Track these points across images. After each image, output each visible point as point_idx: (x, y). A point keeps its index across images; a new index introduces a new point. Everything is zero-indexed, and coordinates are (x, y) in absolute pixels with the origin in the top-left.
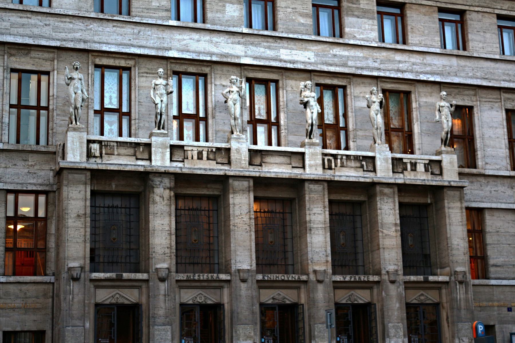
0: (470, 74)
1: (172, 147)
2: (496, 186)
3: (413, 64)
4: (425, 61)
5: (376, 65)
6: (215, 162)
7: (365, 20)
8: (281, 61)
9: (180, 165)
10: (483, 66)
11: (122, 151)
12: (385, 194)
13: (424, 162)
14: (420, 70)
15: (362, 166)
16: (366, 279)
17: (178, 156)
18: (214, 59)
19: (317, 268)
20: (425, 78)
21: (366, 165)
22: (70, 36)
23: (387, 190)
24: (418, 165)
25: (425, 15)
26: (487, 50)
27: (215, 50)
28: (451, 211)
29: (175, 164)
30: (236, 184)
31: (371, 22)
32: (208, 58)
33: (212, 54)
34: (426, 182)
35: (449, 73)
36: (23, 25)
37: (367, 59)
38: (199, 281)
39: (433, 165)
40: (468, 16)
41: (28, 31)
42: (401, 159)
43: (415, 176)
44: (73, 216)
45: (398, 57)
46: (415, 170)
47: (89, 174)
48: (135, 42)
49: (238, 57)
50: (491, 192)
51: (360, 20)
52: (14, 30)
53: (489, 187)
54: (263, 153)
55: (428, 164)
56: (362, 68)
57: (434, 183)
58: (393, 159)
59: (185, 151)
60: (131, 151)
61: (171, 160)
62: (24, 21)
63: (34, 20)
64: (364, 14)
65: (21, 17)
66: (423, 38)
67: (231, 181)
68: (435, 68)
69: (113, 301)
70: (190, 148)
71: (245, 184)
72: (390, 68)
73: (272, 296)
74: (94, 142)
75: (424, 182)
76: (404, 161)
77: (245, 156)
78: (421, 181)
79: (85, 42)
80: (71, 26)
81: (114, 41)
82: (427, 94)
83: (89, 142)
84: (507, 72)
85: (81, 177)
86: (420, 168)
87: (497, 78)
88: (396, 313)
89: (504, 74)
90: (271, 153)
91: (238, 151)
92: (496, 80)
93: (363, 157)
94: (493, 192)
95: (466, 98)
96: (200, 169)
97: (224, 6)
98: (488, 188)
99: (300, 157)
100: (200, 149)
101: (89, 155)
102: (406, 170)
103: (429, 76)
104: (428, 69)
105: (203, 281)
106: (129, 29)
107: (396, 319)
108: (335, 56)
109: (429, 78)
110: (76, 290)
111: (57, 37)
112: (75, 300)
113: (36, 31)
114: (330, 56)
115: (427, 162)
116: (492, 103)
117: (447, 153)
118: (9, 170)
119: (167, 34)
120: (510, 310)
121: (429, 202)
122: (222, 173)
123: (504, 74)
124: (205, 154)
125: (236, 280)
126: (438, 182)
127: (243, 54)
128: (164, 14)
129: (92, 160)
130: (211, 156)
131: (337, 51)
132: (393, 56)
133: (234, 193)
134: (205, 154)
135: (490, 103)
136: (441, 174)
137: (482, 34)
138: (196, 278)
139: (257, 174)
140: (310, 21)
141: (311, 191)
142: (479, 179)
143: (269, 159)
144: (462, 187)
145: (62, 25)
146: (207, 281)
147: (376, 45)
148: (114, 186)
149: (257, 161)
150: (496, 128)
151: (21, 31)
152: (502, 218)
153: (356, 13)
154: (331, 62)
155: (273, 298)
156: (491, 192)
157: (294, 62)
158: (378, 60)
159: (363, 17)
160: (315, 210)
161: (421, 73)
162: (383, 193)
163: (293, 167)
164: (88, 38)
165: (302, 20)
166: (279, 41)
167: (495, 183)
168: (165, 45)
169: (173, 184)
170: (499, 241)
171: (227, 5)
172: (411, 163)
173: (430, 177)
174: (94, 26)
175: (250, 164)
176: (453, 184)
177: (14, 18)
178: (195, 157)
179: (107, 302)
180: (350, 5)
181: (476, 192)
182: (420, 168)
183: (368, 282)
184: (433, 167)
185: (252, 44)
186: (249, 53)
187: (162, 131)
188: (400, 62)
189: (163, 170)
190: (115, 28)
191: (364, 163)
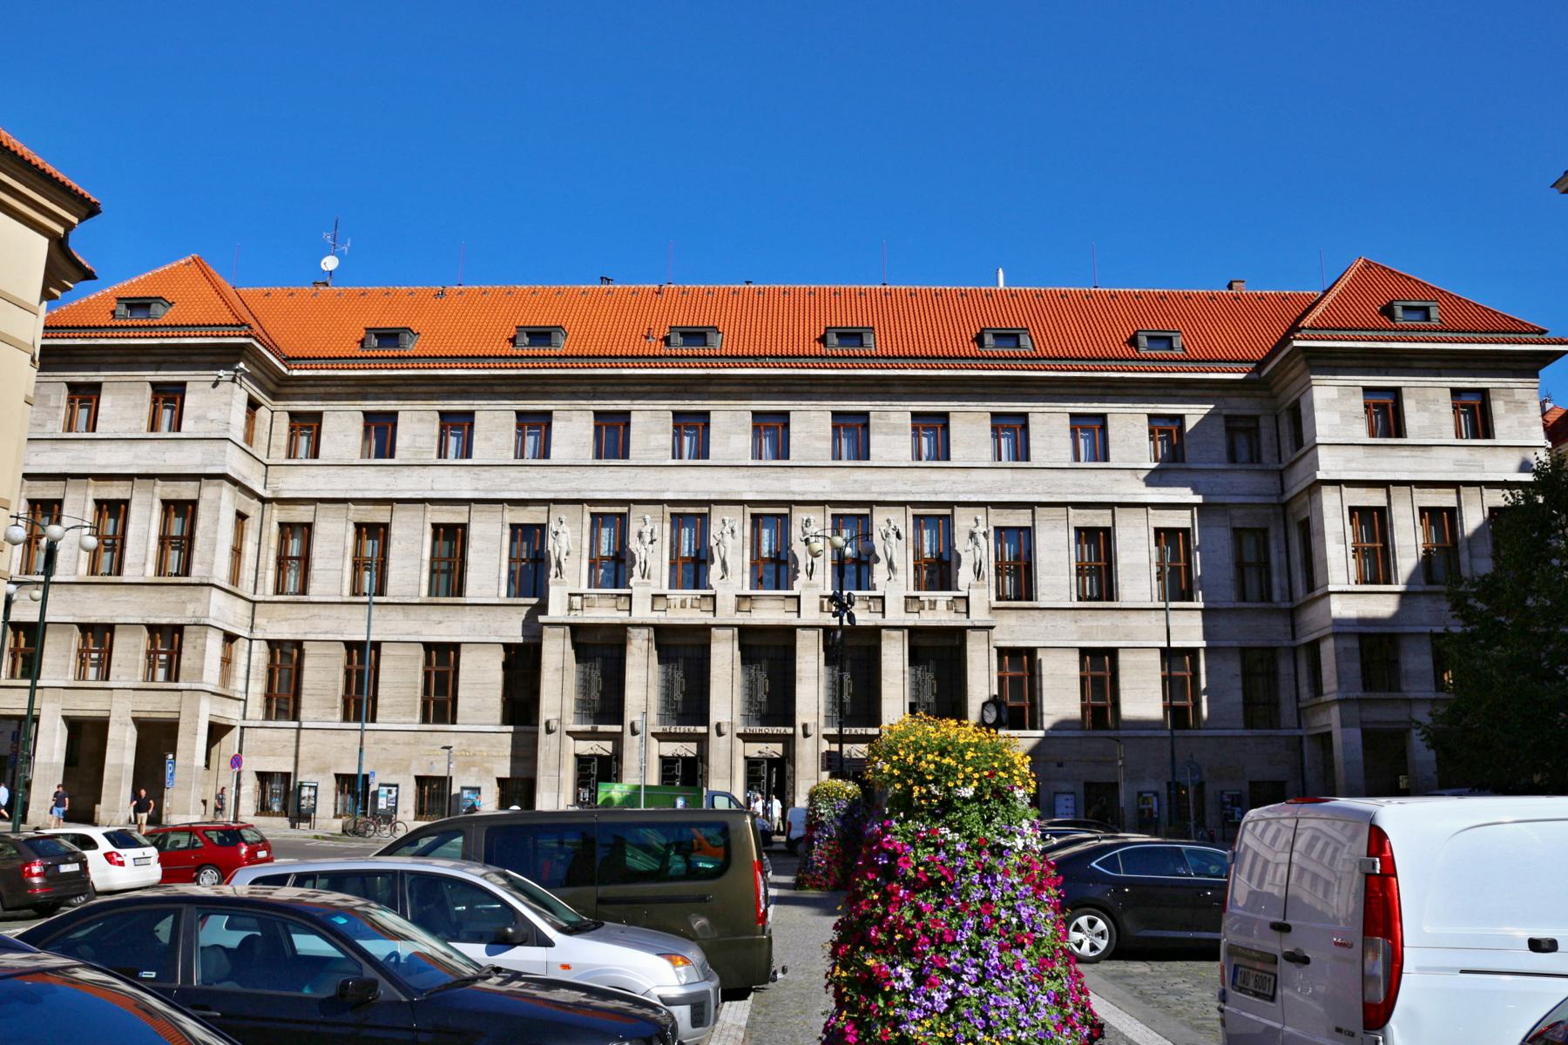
0: (1028, 489)
1: (654, 596)
4: (969, 478)
5: (907, 488)
7: (896, 437)
8: (793, 493)
9: (662, 614)
11: (604, 602)
12: (893, 638)
13: (946, 599)
14: (961, 490)
15: (869, 607)
16: (864, 732)
17: (660, 604)
18: (713, 497)
19: (806, 721)
20: (965, 499)
22: (566, 486)
24: (938, 603)
25: (973, 424)
27: (718, 487)
28: (974, 654)
29: (655, 614)
31: (902, 438)
32: (706, 498)
33: (709, 492)
35: (1000, 490)
36: (522, 479)
37: (895, 481)
38: (675, 733)
39: (957, 601)
40: (1031, 419)
41: (526, 486)
42: (918, 597)
43: (934, 615)
44: (552, 669)
45: (936, 475)
46: (934, 609)
47: (567, 628)
48: (631, 487)
49: (739, 492)
50: (1046, 628)
51: (889, 438)
52: (513, 486)
56: (885, 493)
57: (953, 624)
58: (906, 597)
60: (613, 602)
61: (653, 610)
62: (524, 475)
63: (533, 472)
64: (895, 429)
67: (713, 629)
69: (592, 752)
70: (673, 597)
71: (729, 632)
72: (924, 490)
74: (576, 595)
76: (921, 599)
77: (732, 601)
79: (579, 491)
80: (568, 475)
81: (609, 488)
83: (571, 595)
85: (560, 630)
86: (942, 605)
87: (1064, 491)
89: (1074, 485)
91: (724, 596)
92: (1059, 493)
93: (871, 597)
95: (1022, 517)
96: (679, 619)
97: (729, 438)
98: (1044, 623)
99: (796, 600)
100: (684, 597)
101: (571, 609)
102: (923, 609)
103: (969, 496)
104: (973, 487)
105: (680, 734)
106: (625, 472)
108: (856, 481)
110: (552, 742)
111: (553, 489)
112: (552, 750)
113: (534, 485)
115: (950, 599)
117: (977, 587)
118: (505, 624)
119: (666, 473)
120: (1060, 765)
121: (957, 643)
122: (702, 622)
123: (1074, 485)
124: (689, 602)
125: (713, 732)
127: (748, 489)
128: (663, 453)
129: (573, 613)
130: (696, 604)
131: (859, 474)
133: (718, 641)
134: (689, 602)
136: (968, 612)
137: (1048, 439)
138: (673, 731)
139: (741, 623)
140: (829, 445)
141: (804, 637)
142: (1032, 612)
143: (758, 604)
144: (992, 627)
145: (559, 475)
146: (684, 734)
147: (906, 465)
148: (599, 637)
149: (746, 606)
150: (1059, 551)
151: (520, 486)
153: (884, 430)
154: (850, 489)
155: (760, 752)
156: (1046, 628)
157: (803, 493)
158: (909, 483)
159: (893, 434)
160: (807, 658)
161: (959, 493)
164: (584, 487)
165: (818, 444)
168: (663, 487)
169: (652, 635)
171: (732, 436)
172: (930, 601)
173: (953, 615)
174: (591, 472)
175: (738, 610)
176: (977, 624)
177: (513, 472)
178: (678, 606)
179: (587, 753)
180: (878, 421)
182: (942, 605)
183: (866, 735)
185: (758, 476)
186: (755, 487)
187: (646, 580)
188: (936, 481)
189: (639, 622)
191: (871, 604)
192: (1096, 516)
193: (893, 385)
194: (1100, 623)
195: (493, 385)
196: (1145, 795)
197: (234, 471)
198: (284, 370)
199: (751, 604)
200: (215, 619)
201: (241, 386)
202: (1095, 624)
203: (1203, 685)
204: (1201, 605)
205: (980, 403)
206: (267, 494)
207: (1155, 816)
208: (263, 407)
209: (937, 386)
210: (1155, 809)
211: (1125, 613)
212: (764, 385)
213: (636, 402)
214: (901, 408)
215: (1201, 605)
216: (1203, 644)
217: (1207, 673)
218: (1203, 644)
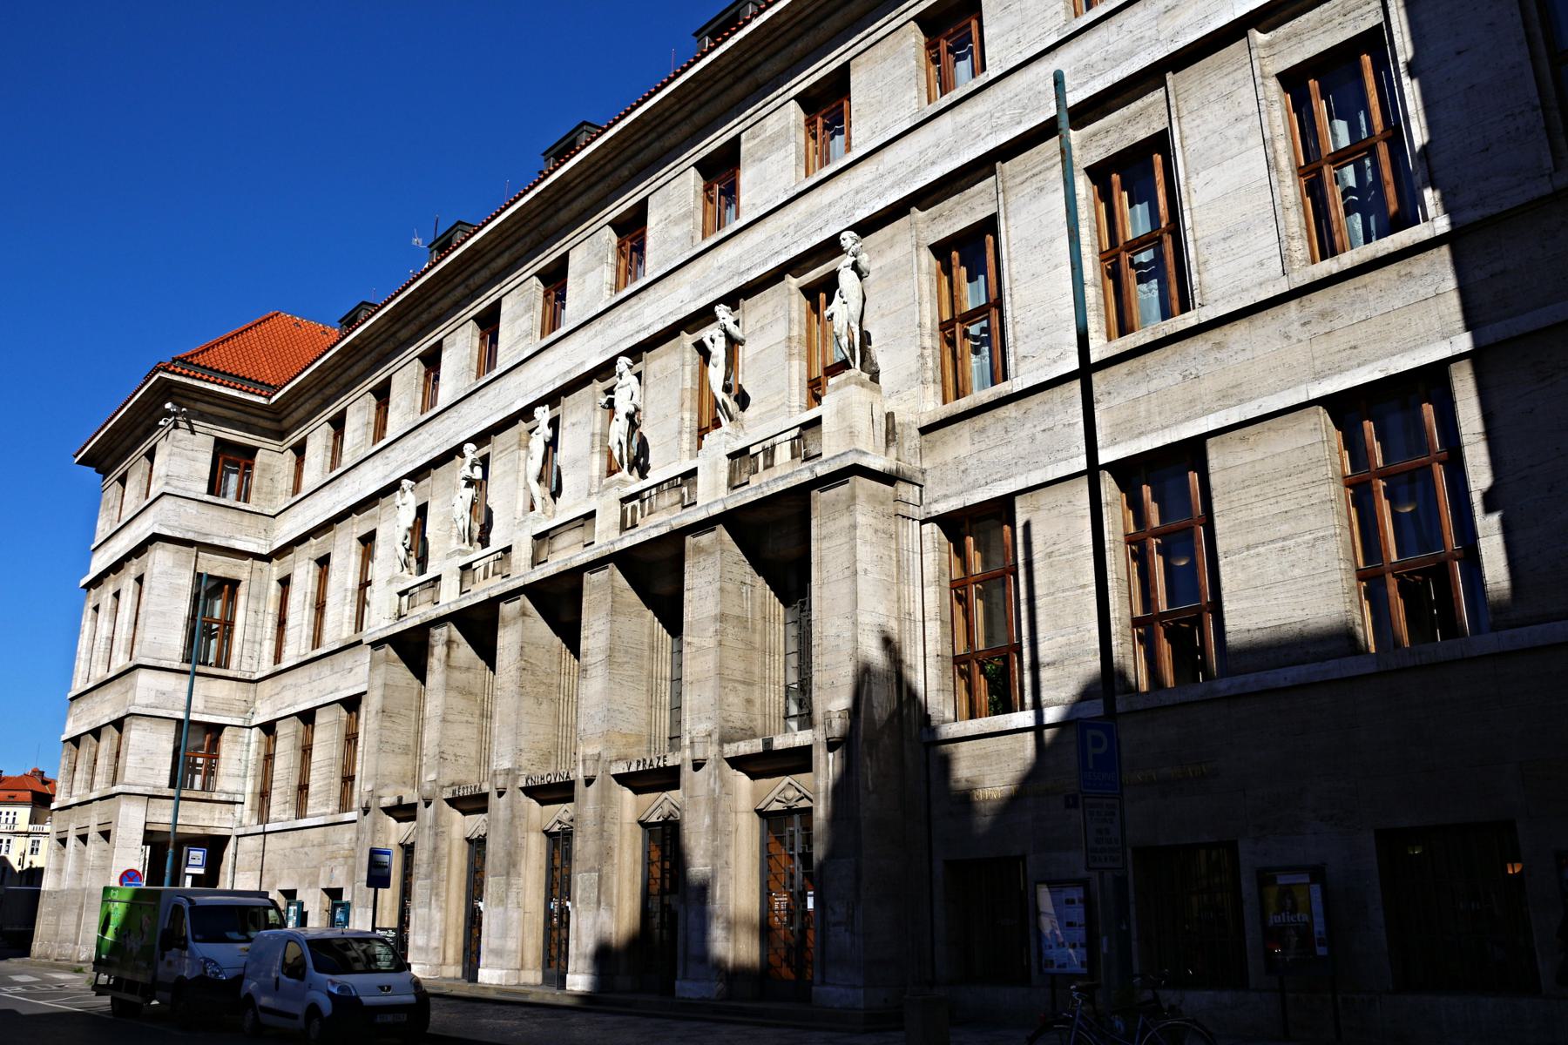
2: (1049, 413)
3: (857, 193)
6: (500, 576)
10: (1018, 90)
21: (689, 494)
23: (705, 539)
26: (1028, 40)
28: (825, 544)
30: (506, 609)
34: (765, 489)
46: (772, 465)
53: (1029, 425)
54: (551, 535)
55: (799, 437)
59: (475, 569)
65: (415, 438)
66: (877, 119)
68: (901, 172)
73: (556, 818)
75: (760, 491)
78: (754, 492)
82: (883, 247)
84: (1084, 62)
88: (703, 842)
90: (559, 530)
94: (1039, 436)
107: (702, 857)
108: (720, 268)
109: (873, 208)
114: (713, 274)
115: (794, 433)
116: (1041, 177)
126: (789, 480)
132: (818, 200)
135: (1034, 180)
142: (1001, 412)
152: (1063, 510)
155: (560, 822)
156: (1033, 439)
162: (699, 547)
163: (585, 546)
166: (643, 295)
167: (1047, 407)
170: (1053, 583)
181: (995, 452)
184: (808, 442)
190: (483, 398)
192: (1129, 120)
193: (758, 66)
194: (1154, 385)
195: (395, 333)
196: (1282, 880)
197: (168, 527)
198: (262, 400)
199: (550, 544)
200: (147, 706)
201: (193, 432)
202: (1143, 390)
203: (1479, 476)
204: (1442, 225)
205: (893, 14)
206: (265, 551)
207: (1321, 951)
208: (260, 451)
209: (815, 25)
210: (1319, 927)
211: (1215, 335)
212: (610, 173)
213: (504, 283)
214: (779, 101)
215: (1442, 225)
216: (1464, 343)
217: (1491, 434)
218: (1464, 343)
